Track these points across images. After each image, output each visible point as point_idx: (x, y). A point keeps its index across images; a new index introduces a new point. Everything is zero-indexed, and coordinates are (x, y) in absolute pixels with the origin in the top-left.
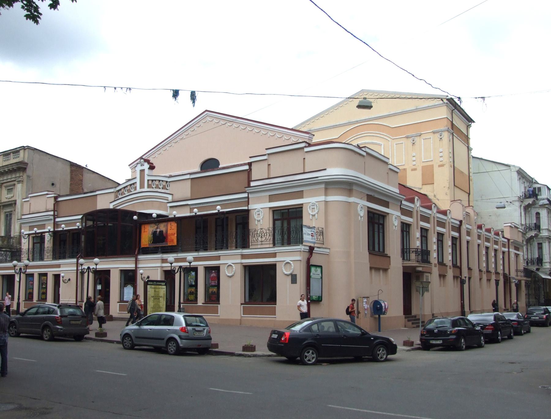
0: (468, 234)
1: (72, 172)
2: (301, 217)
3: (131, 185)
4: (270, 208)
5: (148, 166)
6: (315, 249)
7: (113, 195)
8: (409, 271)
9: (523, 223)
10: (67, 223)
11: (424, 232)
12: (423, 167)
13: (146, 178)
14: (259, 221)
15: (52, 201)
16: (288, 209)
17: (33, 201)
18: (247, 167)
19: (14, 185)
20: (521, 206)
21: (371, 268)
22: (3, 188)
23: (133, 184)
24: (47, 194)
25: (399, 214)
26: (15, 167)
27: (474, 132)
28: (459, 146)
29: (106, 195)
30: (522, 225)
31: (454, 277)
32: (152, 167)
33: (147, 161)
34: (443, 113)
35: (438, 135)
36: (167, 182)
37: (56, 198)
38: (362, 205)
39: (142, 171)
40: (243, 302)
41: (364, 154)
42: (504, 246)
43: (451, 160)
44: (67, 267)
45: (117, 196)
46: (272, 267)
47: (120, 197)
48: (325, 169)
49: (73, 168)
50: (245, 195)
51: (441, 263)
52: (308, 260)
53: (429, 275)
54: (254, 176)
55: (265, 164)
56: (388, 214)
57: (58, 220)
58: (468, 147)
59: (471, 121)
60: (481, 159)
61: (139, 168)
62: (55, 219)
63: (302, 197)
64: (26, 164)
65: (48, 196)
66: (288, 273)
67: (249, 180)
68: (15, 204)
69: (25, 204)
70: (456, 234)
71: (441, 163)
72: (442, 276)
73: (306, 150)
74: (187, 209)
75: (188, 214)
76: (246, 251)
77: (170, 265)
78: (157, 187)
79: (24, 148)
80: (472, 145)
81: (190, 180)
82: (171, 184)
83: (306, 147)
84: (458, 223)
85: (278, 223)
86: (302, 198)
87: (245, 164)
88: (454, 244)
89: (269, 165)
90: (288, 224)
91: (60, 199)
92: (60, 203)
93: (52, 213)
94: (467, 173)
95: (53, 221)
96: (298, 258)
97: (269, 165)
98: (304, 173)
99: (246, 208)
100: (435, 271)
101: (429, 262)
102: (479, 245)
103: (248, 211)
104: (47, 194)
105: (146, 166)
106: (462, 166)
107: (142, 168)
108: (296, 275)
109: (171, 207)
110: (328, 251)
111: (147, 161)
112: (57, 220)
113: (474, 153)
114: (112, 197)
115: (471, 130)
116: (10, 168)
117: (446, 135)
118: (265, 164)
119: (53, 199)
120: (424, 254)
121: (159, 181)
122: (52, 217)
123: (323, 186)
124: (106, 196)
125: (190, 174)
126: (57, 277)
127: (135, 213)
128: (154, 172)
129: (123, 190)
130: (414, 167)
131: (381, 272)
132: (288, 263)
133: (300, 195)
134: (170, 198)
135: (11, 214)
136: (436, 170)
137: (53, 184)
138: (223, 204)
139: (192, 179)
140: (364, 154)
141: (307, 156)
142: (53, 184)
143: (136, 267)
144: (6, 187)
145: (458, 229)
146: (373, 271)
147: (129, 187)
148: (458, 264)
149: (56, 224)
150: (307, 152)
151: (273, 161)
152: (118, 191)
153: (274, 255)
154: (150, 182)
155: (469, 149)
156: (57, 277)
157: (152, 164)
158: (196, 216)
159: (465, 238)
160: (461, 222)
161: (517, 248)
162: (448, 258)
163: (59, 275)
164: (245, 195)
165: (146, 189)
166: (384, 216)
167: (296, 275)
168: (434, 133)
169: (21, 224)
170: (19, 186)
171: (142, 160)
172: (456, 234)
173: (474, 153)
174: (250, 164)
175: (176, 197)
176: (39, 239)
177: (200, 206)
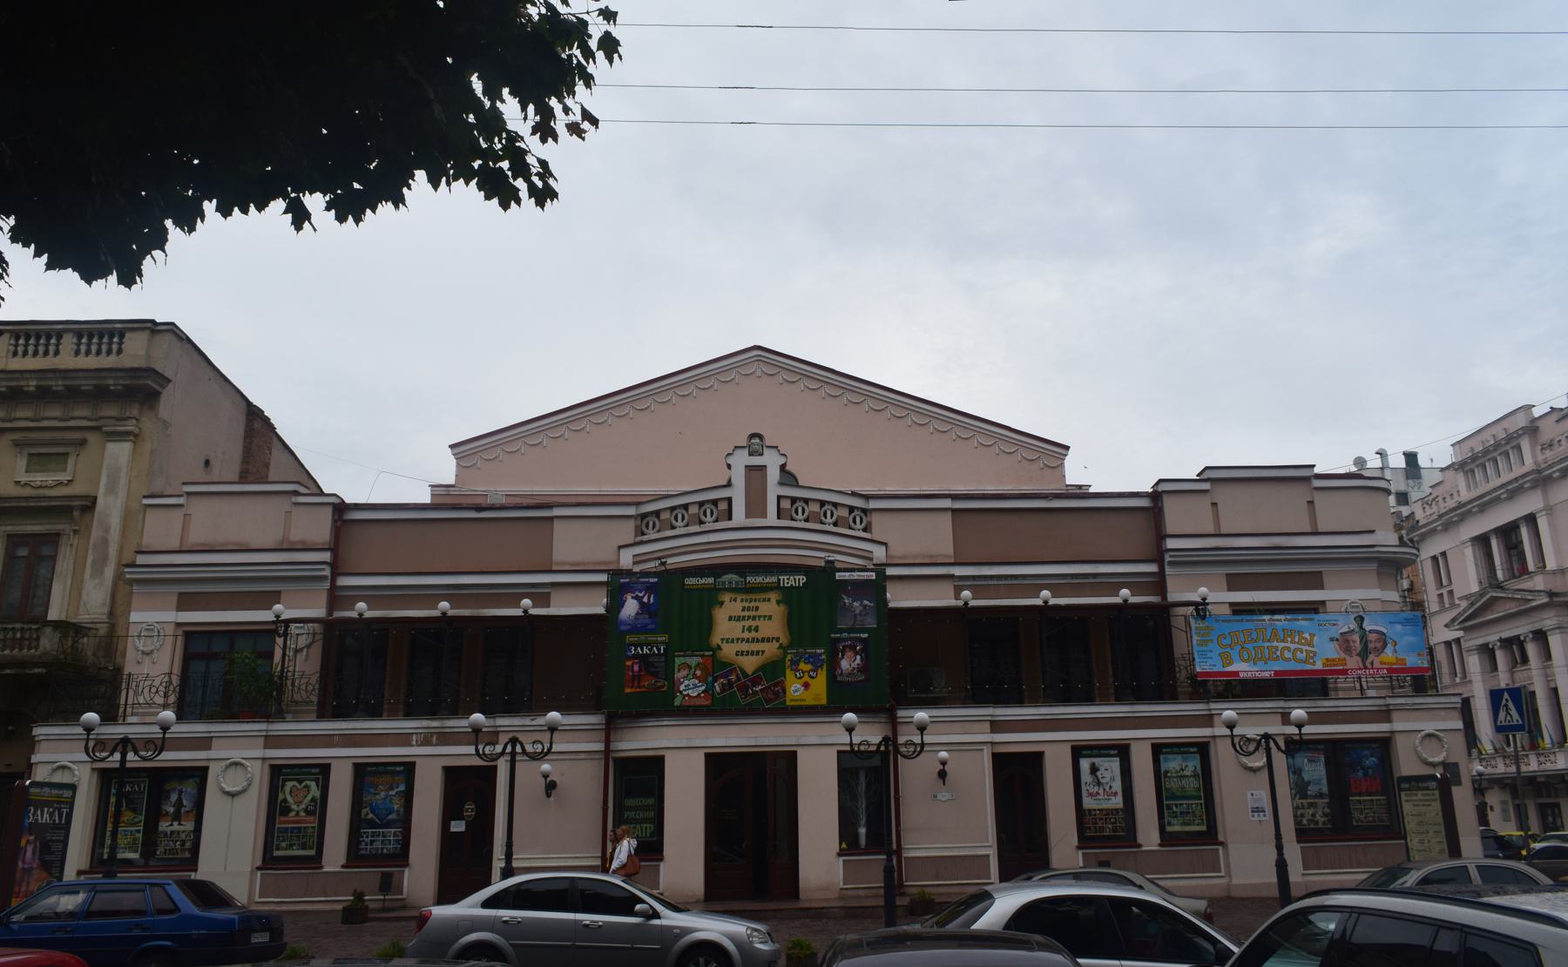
7: (631, 525)
10: (375, 596)
24: (296, 493)
45: (640, 532)
48: (1372, 532)
54: (1171, 526)
57: (344, 581)
63: (1321, 586)
65: (294, 499)
67: (1161, 536)
74: (948, 588)
75: (952, 602)
77: (1227, 732)
95: (327, 585)
97: (1214, 504)
104: (296, 493)
107: (756, 461)
108: (1456, 765)
112: (344, 581)
114: (627, 532)
121: (823, 503)
122: (327, 572)
123: (1374, 566)
124: (596, 527)
125: (955, 497)
133: (1315, 581)
137: (207, 463)
138: (1060, 585)
139: (954, 511)
141: (1319, 498)
142: (207, 463)
149: (336, 598)
154: (786, 504)
158: (965, 612)
167: (1456, 765)
177: (980, 585)
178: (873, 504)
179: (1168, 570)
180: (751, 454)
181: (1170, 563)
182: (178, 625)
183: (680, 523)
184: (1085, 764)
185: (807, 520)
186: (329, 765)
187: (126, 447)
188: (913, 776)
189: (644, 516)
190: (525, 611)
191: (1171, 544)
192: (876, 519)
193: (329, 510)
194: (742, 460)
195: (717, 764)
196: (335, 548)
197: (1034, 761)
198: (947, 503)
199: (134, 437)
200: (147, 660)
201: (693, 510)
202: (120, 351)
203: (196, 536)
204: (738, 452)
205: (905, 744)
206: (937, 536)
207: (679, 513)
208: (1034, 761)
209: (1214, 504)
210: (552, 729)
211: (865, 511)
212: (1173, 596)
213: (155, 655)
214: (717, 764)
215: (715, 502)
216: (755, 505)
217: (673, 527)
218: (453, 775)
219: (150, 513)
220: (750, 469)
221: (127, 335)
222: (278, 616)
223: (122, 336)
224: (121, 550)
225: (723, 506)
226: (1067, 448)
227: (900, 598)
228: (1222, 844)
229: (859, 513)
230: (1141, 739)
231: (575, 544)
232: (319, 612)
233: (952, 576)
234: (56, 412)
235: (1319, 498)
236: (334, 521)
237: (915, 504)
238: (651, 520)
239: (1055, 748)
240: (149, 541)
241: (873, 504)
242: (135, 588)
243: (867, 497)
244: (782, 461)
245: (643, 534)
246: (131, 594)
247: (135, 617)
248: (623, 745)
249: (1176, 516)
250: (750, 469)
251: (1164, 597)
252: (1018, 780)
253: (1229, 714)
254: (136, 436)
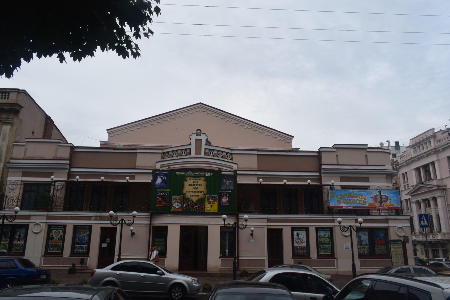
10: (82, 174)
24: (59, 143)
29: (150, 155)
54: (324, 161)
57: (73, 170)
65: (59, 144)
67: (321, 165)
74: (255, 178)
76: (369, 217)
77: (339, 225)
86: (369, 182)
95: (68, 171)
97: (337, 155)
104: (59, 143)
107: (199, 137)
112: (73, 170)
114: (159, 158)
121: (218, 151)
122: (68, 167)
124: (150, 155)
125: (259, 151)
137: (33, 133)
138: (289, 178)
139: (258, 155)
142: (33, 133)
149: (70, 175)
150: (368, 152)
154: (207, 151)
177: (265, 177)
178: (234, 152)
179: (322, 175)
180: (197, 135)
181: (323, 173)
182: (22, 181)
183: (175, 156)
184: (295, 233)
185: (213, 156)
186: (66, 225)
187: (9, 127)
188: (243, 234)
189: (164, 153)
190: (127, 181)
191: (323, 167)
192: (234, 156)
193: (69, 148)
194: (194, 137)
195: (184, 229)
196: (70, 159)
197: (280, 231)
199: (12, 124)
200: (12, 192)
201: (179, 152)
202: (8, 98)
203: (29, 154)
204: (193, 135)
205: (241, 225)
206: (253, 162)
207: (175, 152)
208: (280, 231)
209: (337, 155)
210: (134, 216)
211: (231, 154)
212: (323, 183)
213: (14, 190)
214: (184, 229)
215: (186, 150)
216: (198, 151)
217: (173, 157)
218: (103, 230)
219: (15, 147)
220: (197, 140)
221: (11, 93)
222: (52, 180)
223: (9, 93)
224: (6, 158)
225: (188, 151)
226: (293, 137)
227: (241, 181)
228: (336, 258)
229: (229, 154)
230: (312, 226)
231: (143, 161)
232: (65, 179)
233: (257, 175)
235: (369, 155)
236: (71, 151)
237: (247, 152)
238: (166, 154)
239: (286, 227)
240: (14, 155)
241: (234, 152)
242: (9, 170)
243: (232, 150)
244: (207, 138)
245: (164, 158)
246: (8, 171)
247: (9, 178)
248: (155, 222)
249: (325, 159)
250: (197, 140)
251: (321, 183)
252: (275, 237)
253: (339, 219)
254: (12, 124)
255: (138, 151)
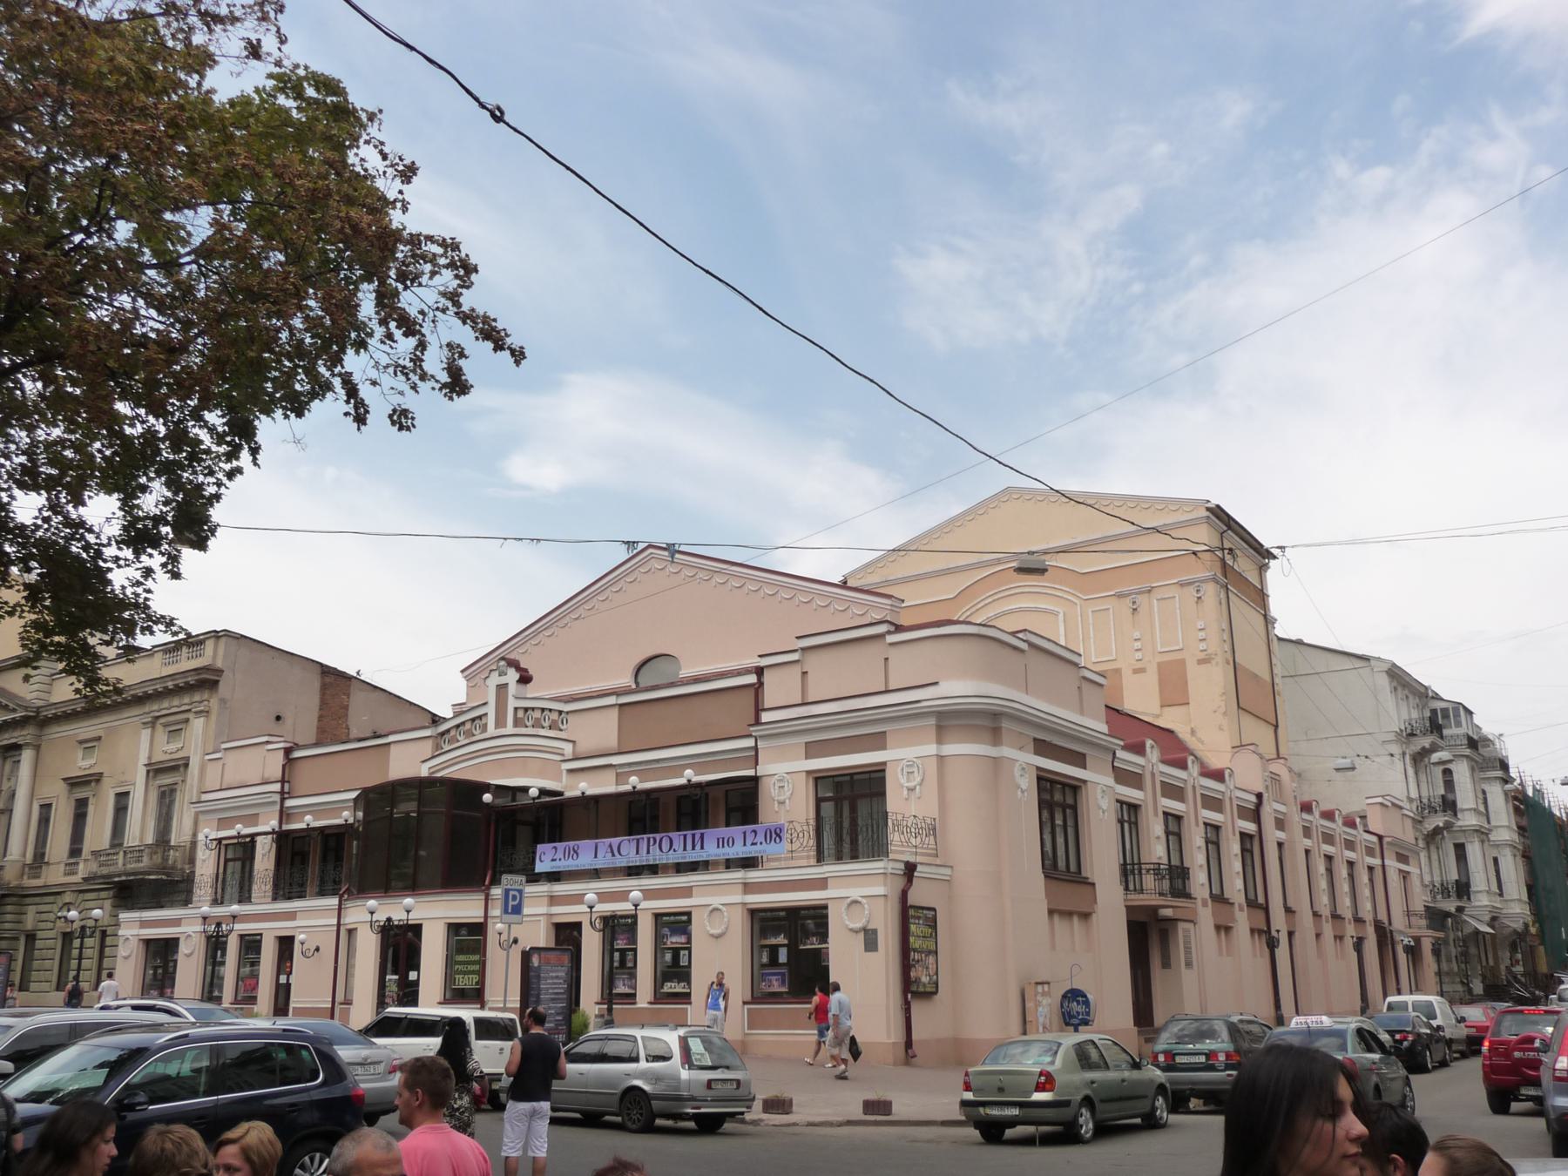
0: (1280, 824)
1: (324, 688)
2: (882, 794)
3: (473, 720)
4: (809, 773)
5: (517, 676)
6: (919, 868)
7: (430, 743)
8: (1142, 918)
9: (1414, 794)
10: (315, 810)
11: (1174, 824)
12: (1159, 664)
13: (512, 703)
14: (782, 803)
15: (279, 758)
16: (851, 775)
17: (231, 758)
18: (752, 679)
19: (187, 721)
20: (1404, 754)
21: (1051, 912)
22: (159, 728)
23: (480, 717)
25: (1110, 781)
26: (191, 679)
27: (1276, 579)
28: (1244, 613)
30: (1410, 800)
31: (1252, 931)
32: (525, 679)
33: (514, 664)
34: (1204, 536)
35: (1191, 589)
36: (560, 712)
37: (288, 751)
38: (1024, 763)
39: (502, 688)
40: (748, 998)
41: (1024, 646)
42: (1370, 852)
43: (1227, 647)
44: (312, 918)
45: (438, 747)
46: (818, 915)
47: (446, 748)
49: (328, 680)
50: (750, 743)
51: (1219, 899)
52: (904, 895)
53: (1190, 926)
54: (769, 699)
55: (796, 672)
56: (1085, 782)
57: (289, 803)
58: (1265, 616)
59: (1269, 555)
60: (1299, 642)
61: (495, 680)
62: (283, 800)
63: (882, 746)
64: (220, 672)
65: (270, 747)
66: (859, 925)
67: (758, 709)
68: (186, 765)
69: (211, 767)
70: (1250, 827)
71: (1202, 655)
72: (1223, 929)
73: (890, 639)
74: (610, 776)
78: (537, 724)
79: (216, 635)
80: (1275, 609)
81: (616, 710)
82: (570, 718)
83: (889, 632)
84: (1253, 799)
85: (828, 808)
87: (747, 671)
88: (1246, 851)
89: (805, 673)
90: (852, 810)
91: (297, 754)
92: (299, 764)
93: (277, 787)
94: (1267, 677)
96: (881, 890)
97: (805, 673)
98: (887, 691)
99: (751, 773)
100: (1206, 916)
101: (1188, 896)
102: (1307, 852)
103: (755, 780)
105: (512, 676)
106: (1253, 660)
107: (503, 680)
108: (875, 931)
109: (570, 771)
110: (948, 871)
111: (514, 664)
113: (1280, 631)
114: (427, 748)
115: (1271, 576)
116: (181, 682)
117: (1210, 590)
118: (797, 670)
119: (282, 753)
120: (1177, 876)
122: (277, 798)
123: (932, 721)
126: (286, 945)
127: (486, 787)
128: (531, 690)
129: (453, 733)
130: (1139, 665)
131: (1075, 919)
132: (856, 902)
134: (568, 749)
135: (173, 791)
136: (1192, 670)
137: (278, 718)
138: (699, 763)
139: (621, 705)
140: (1024, 646)
141: (893, 654)
142: (278, 718)
143: (486, 917)
144: (165, 725)
145: (1255, 814)
146: (1056, 918)
147: (468, 726)
148: (1261, 900)
149: (284, 815)
151: (814, 663)
152: (443, 734)
153: (822, 883)
154: (520, 714)
155: (1268, 621)
156: (286, 945)
157: (526, 670)
159: (1272, 835)
160: (1259, 796)
161: (1402, 858)
162: (1235, 887)
163: (291, 939)
164: (750, 743)
165: (510, 729)
166: (1074, 788)
167: (875, 931)
168: (1182, 585)
169: (197, 814)
170: (198, 724)
171: (502, 663)
172: (1250, 827)
173: (1280, 631)
174: (759, 671)
175: (585, 746)
176: (244, 850)
177: (642, 769)
198: (612, 700)
199: (206, 713)
203: (229, 779)
234: (176, 702)
240: (209, 786)
249: (778, 689)
255: (391, 738)
